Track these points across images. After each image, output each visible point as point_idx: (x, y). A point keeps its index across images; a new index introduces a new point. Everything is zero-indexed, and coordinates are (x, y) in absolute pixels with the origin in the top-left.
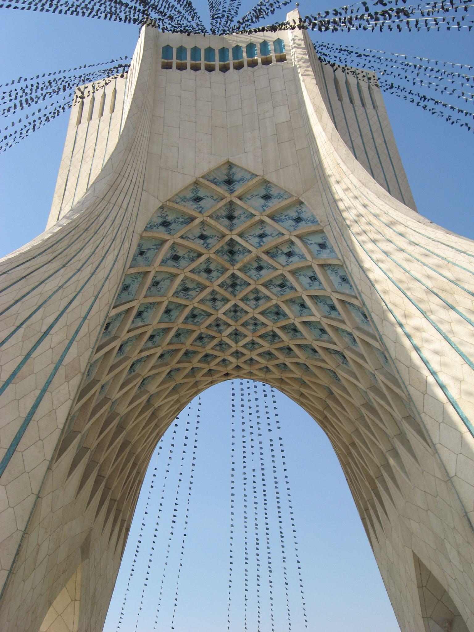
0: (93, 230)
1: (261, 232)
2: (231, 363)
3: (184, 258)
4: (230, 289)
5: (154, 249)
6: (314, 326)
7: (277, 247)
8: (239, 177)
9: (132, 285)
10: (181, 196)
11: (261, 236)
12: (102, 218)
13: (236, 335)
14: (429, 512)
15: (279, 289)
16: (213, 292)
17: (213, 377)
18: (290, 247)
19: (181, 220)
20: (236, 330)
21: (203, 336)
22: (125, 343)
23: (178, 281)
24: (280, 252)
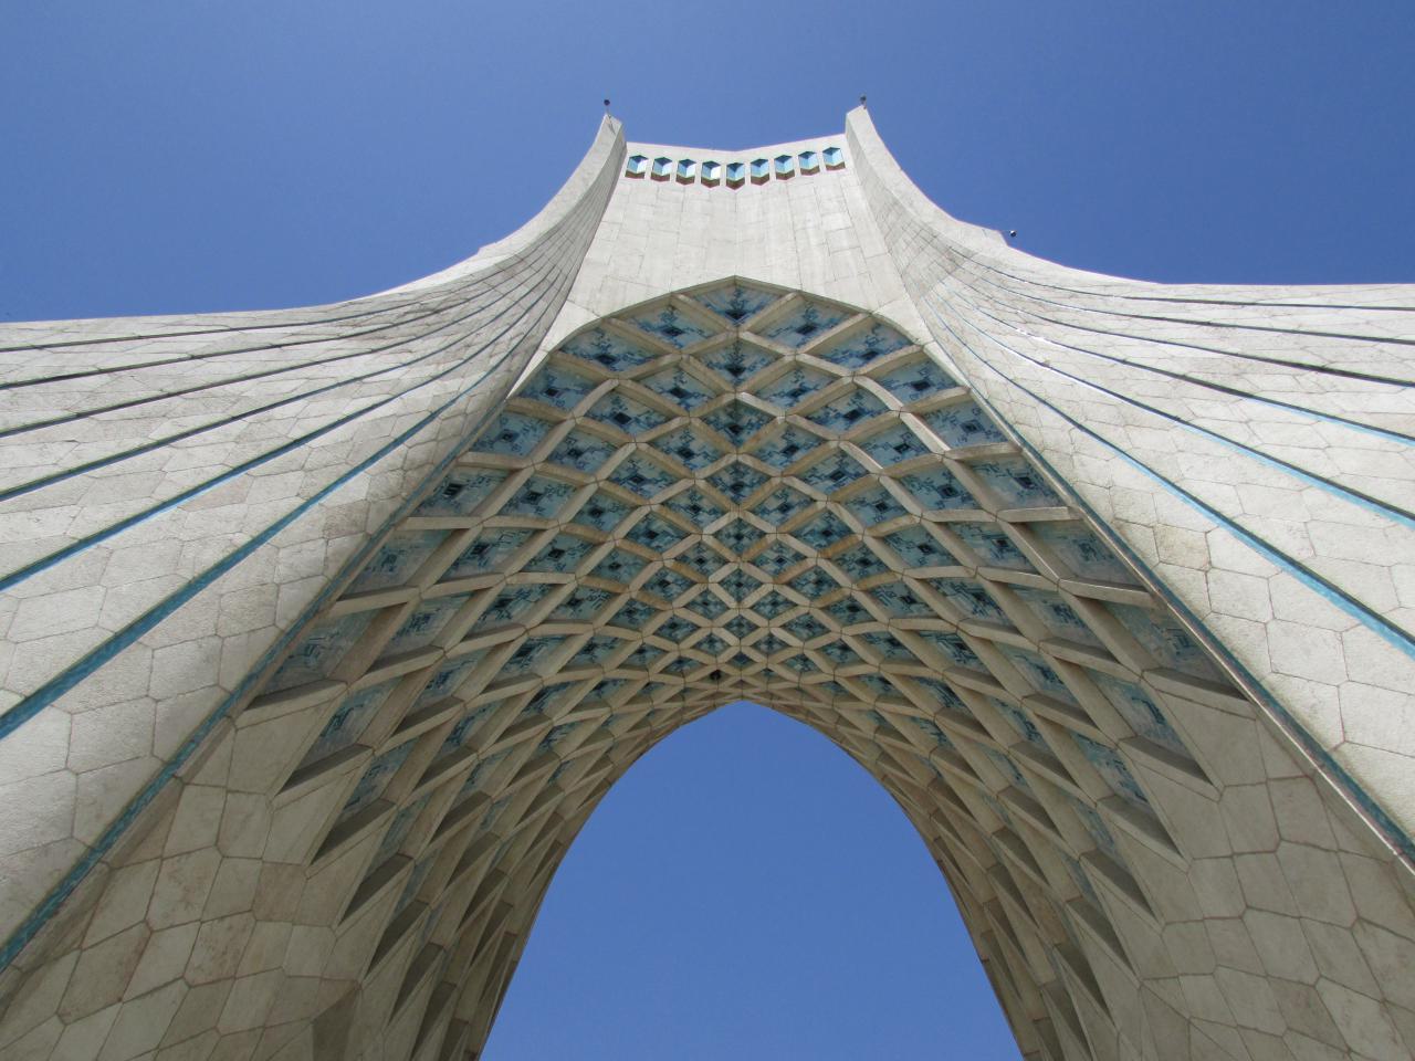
0: (451, 316)
1: (797, 386)
3: (637, 421)
4: (730, 494)
5: (577, 392)
6: (907, 543)
7: (827, 407)
8: (755, 306)
9: (521, 436)
10: (641, 321)
11: (795, 394)
12: (473, 306)
13: (739, 585)
14: (1250, 916)
15: (830, 483)
16: (692, 493)
17: (688, 679)
18: (854, 403)
19: (637, 357)
20: (739, 573)
21: (669, 578)
22: (494, 545)
23: (620, 456)
24: (832, 414)
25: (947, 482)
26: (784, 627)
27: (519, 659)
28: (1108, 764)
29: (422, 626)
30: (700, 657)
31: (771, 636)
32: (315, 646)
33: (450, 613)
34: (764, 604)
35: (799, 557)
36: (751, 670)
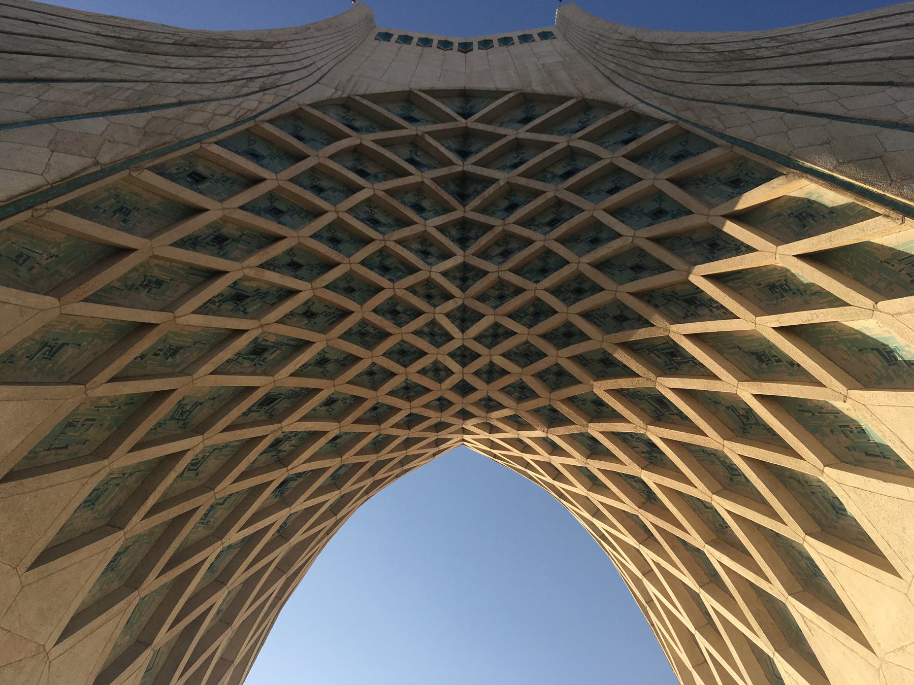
2: (450, 373)
13: (465, 318)
18: (569, 165)
21: (398, 308)
22: (234, 240)
25: (658, 206)
26: (503, 355)
27: (252, 356)
28: (832, 432)
29: (154, 290)
30: (426, 382)
31: (491, 364)
32: (29, 257)
33: (184, 288)
34: (485, 336)
35: (519, 291)
36: (474, 397)
